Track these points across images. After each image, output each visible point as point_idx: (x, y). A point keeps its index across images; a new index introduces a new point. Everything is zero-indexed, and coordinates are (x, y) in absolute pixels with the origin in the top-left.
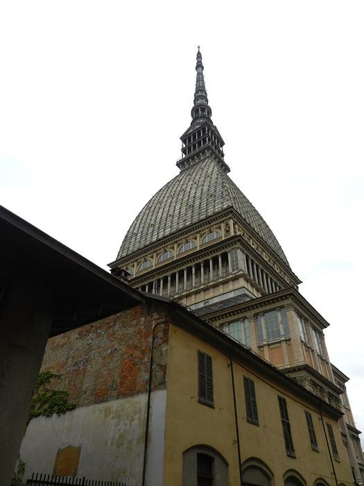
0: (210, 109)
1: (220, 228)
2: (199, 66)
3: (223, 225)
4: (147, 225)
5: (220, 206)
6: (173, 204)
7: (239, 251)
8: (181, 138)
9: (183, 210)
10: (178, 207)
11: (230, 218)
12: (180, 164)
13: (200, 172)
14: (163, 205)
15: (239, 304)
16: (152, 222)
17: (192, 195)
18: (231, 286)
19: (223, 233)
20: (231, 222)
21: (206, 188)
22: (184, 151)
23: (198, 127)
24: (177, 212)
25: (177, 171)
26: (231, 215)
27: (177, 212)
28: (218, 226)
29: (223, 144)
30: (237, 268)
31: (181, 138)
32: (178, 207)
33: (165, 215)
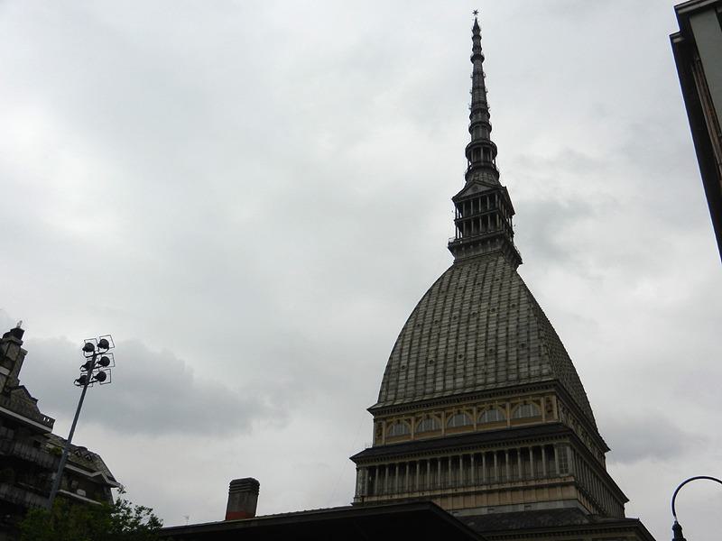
0: (496, 149)
1: (538, 402)
2: (477, 57)
3: (542, 400)
4: (422, 360)
5: (537, 368)
6: (462, 337)
7: (568, 449)
8: (454, 199)
9: (481, 354)
10: (471, 345)
11: (553, 393)
12: (453, 247)
13: (496, 289)
14: (444, 330)
15: (575, 525)
16: (431, 357)
17: (492, 333)
18: (558, 493)
19: (543, 412)
20: (554, 398)
21: (512, 326)
22: (458, 223)
23: (483, 189)
24: (471, 353)
25: (449, 259)
26: (553, 390)
27: (471, 353)
28: (536, 399)
29: (512, 212)
30: (567, 471)
31: (454, 199)
32: (471, 345)
33: (451, 352)
